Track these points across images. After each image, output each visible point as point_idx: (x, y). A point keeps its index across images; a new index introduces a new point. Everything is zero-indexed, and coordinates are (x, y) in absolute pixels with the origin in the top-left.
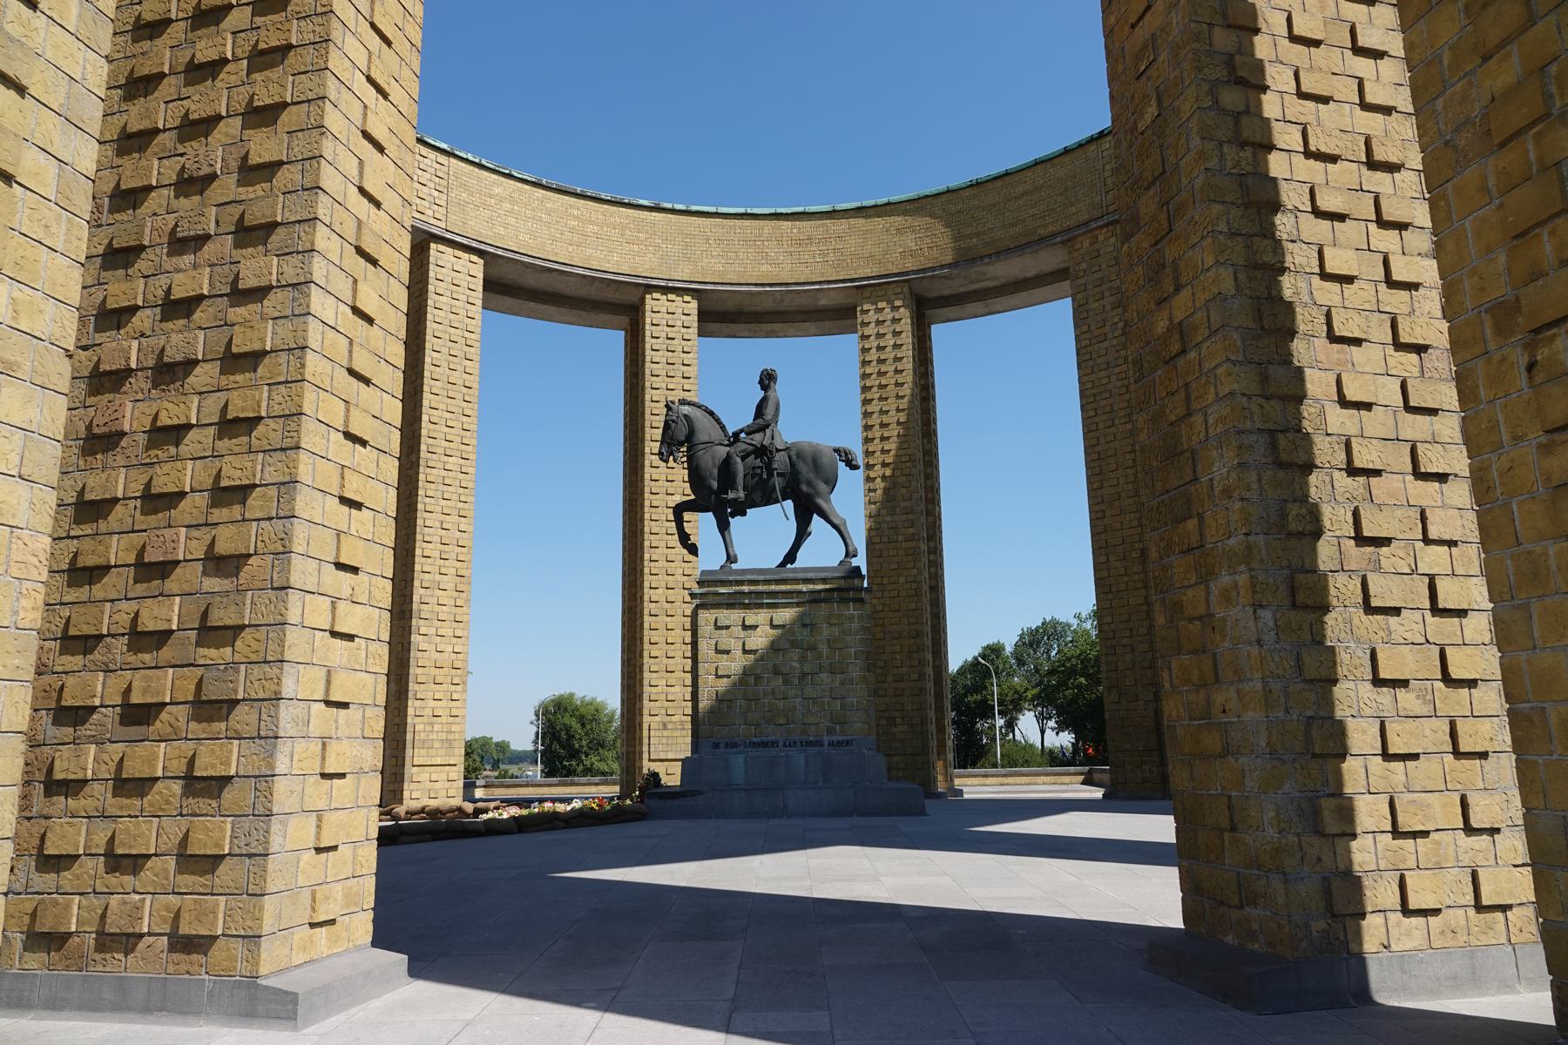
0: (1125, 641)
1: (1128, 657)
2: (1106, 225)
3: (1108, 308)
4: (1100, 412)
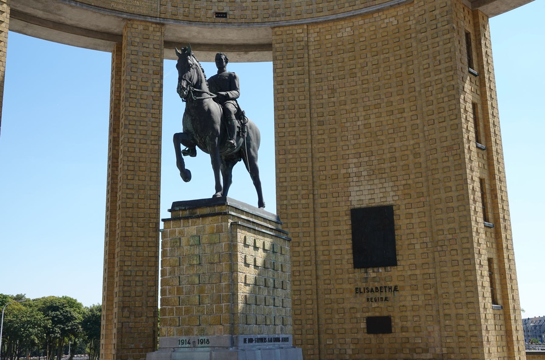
0: (138, 278)
1: (138, 289)
2: (156, 23)
3: (151, 72)
4: (138, 132)
